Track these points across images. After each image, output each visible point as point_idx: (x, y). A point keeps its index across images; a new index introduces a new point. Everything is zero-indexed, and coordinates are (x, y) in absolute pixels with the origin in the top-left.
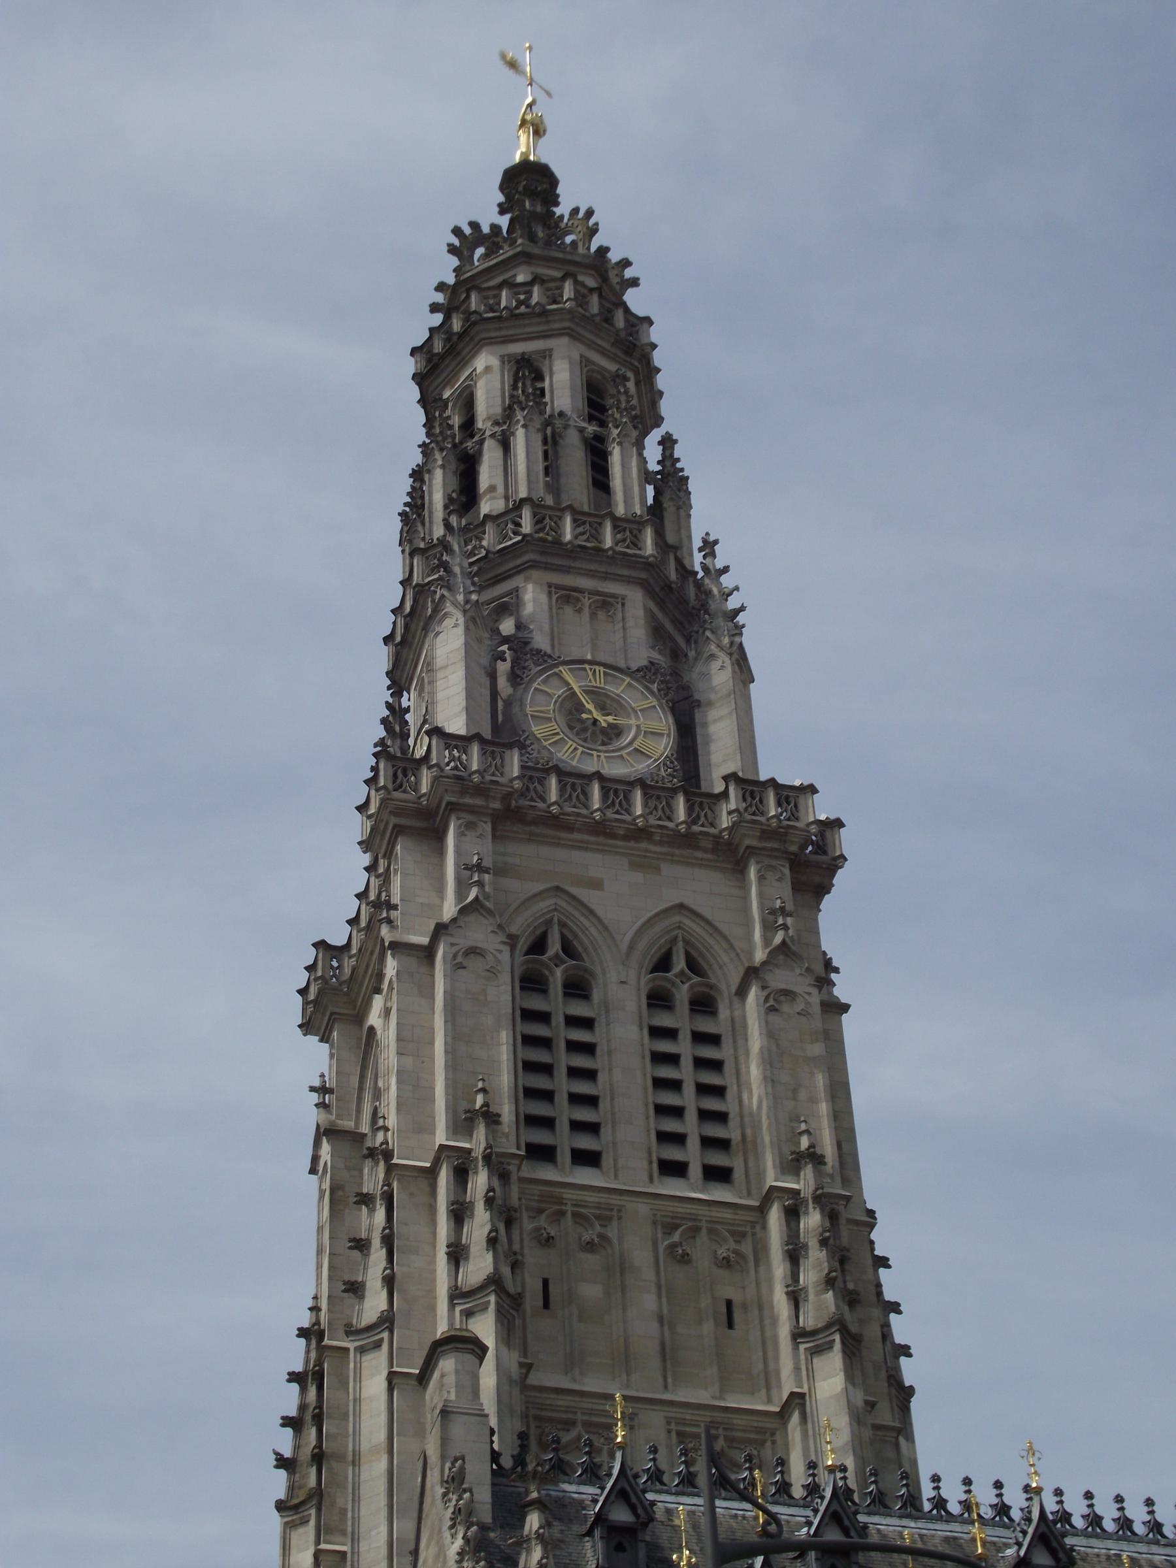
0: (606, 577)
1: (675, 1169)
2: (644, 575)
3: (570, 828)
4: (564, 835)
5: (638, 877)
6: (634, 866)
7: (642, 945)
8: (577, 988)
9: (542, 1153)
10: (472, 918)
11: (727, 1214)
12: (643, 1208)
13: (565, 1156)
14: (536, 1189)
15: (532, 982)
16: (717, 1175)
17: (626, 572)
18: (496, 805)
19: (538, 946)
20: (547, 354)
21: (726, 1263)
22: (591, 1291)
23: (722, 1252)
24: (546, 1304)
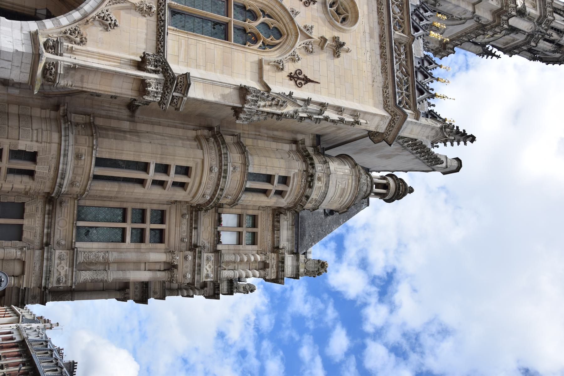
0: (540, 8)
2: (543, 15)
17: (542, 12)
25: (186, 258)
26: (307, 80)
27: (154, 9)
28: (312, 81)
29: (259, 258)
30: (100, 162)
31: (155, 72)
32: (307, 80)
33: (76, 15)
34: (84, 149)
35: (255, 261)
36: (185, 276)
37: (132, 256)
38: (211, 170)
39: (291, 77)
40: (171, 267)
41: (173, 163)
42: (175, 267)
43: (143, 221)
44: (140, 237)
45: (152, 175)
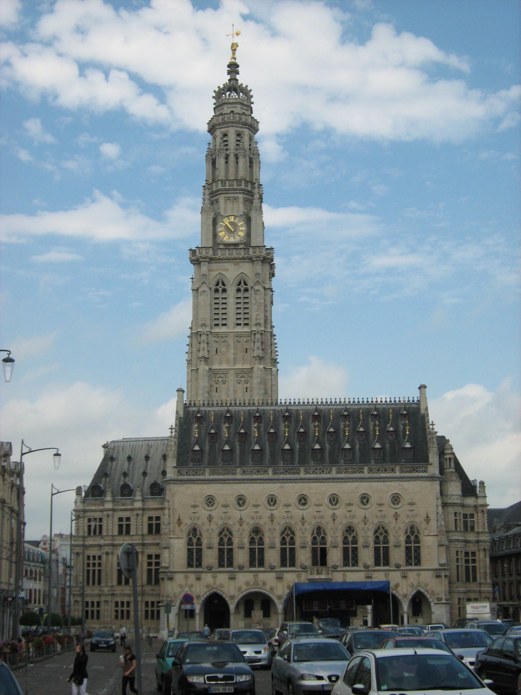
0: (235, 193)
1: (240, 324)
3: (223, 260)
4: (222, 261)
5: (235, 267)
6: (235, 265)
7: (235, 281)
8: (224, 291)
9: (217, 325)
10: (203, 285)
11: (246, 333)
12: (232, 334)
13: (220, 325)
14: (215, 333)
15: (217, 291)
16: (246, 324)
18: (208, 260)
19: (217, 284)
20: (228, 131)
21: (246, 342)
22: (224, 349)
23: (245, 339)
24: (217, 353)
25: (481, 545)
26: (427, 517)
27: (419, 572)
28: (427, 515)
29: (480, 515)
30: (458, 580)
31: (441, 573)
32: (427, 517)
33: (426, 593)
34: (455, 585)
35: (481, 516)
36: (487, 545)
37: (482, 564)
38: (456, 545)
39: (428, 523)
40: (484, 550)
41: (456, 557)
42: (484, 548)
43: (468, 560)
44: (474, 561)
45: (459, 564)
